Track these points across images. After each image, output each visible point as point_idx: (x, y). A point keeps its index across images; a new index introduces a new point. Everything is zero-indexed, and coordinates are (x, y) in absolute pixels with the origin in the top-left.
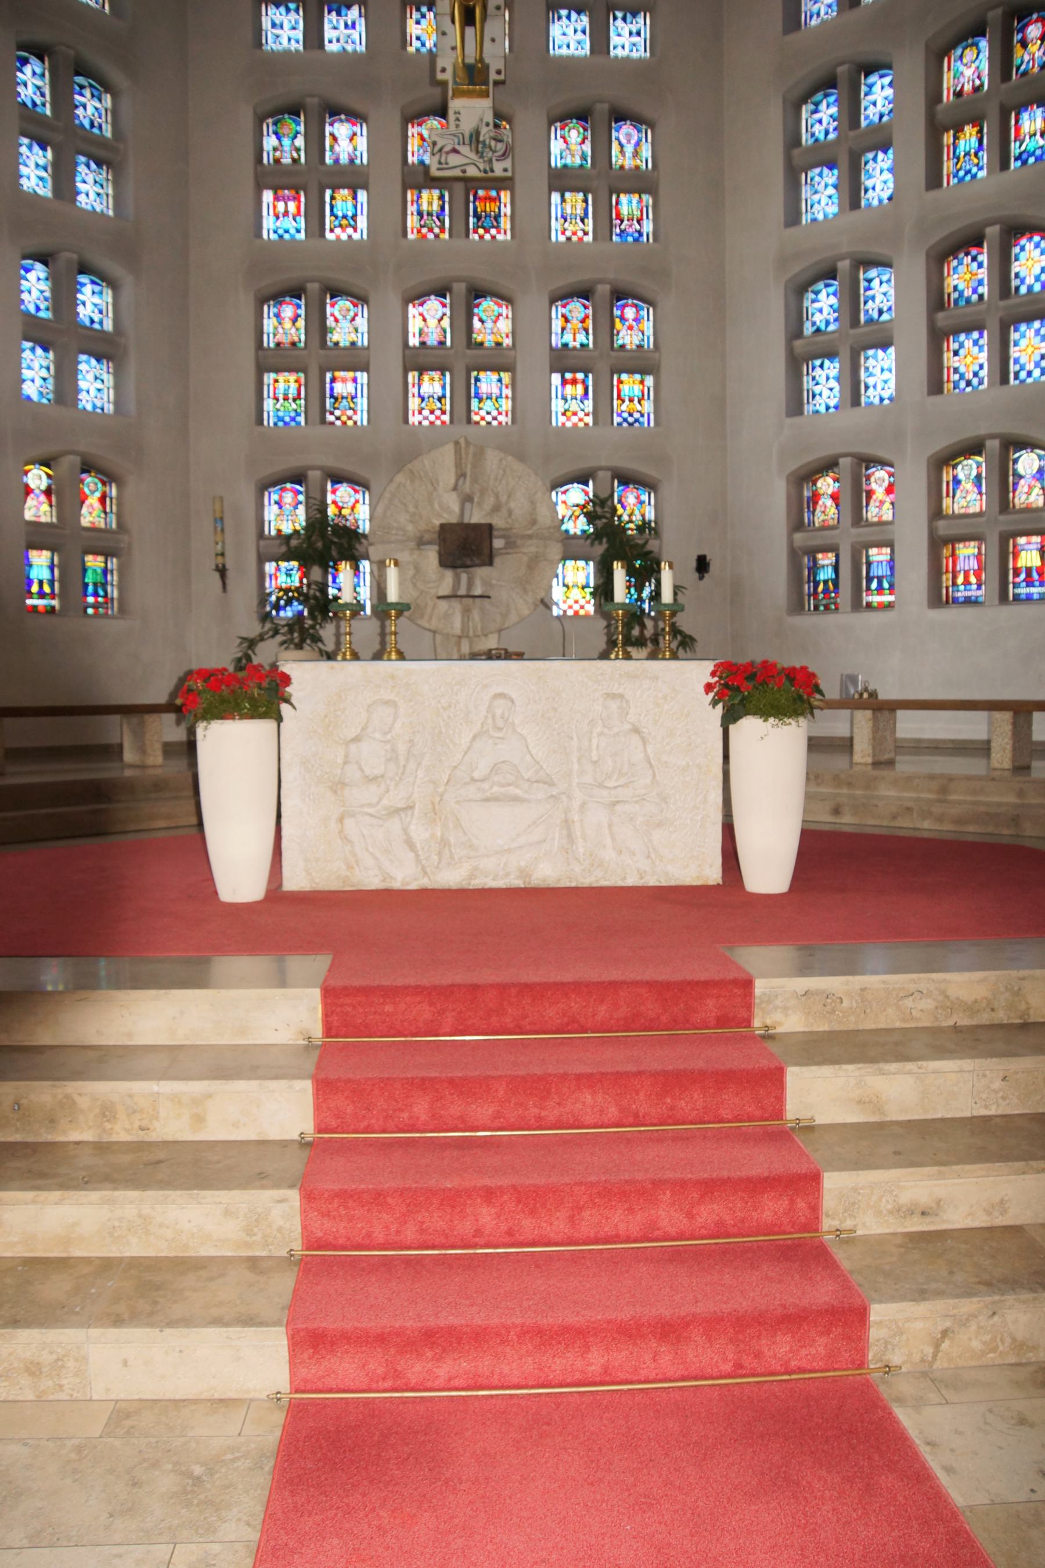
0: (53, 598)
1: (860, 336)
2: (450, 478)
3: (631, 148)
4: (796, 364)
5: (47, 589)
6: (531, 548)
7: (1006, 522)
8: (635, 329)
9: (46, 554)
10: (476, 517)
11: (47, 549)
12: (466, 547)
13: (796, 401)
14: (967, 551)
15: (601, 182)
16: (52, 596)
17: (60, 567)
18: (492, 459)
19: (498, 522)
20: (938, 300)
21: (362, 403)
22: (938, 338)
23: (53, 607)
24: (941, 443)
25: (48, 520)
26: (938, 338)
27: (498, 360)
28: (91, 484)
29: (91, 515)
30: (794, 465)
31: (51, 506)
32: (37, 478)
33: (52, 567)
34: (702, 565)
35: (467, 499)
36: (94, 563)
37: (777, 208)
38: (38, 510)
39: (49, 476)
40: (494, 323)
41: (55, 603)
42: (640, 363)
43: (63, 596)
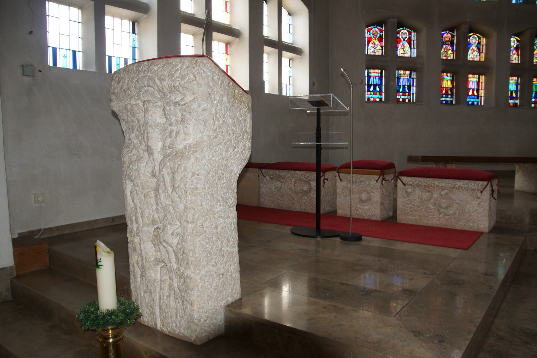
0: (517, 100)
5: (514, 95)
9: (515, 78)
11: (515, 76)
16: (516, 98)
17: (520, 84)
23: (516, 104)
25: (517, 62)
31: (518, 55)
32: (514, 42)
33: (517, 85)
38: (515, 58)
39: (518, 41)
41: (517, 102)
43: (521, 98)
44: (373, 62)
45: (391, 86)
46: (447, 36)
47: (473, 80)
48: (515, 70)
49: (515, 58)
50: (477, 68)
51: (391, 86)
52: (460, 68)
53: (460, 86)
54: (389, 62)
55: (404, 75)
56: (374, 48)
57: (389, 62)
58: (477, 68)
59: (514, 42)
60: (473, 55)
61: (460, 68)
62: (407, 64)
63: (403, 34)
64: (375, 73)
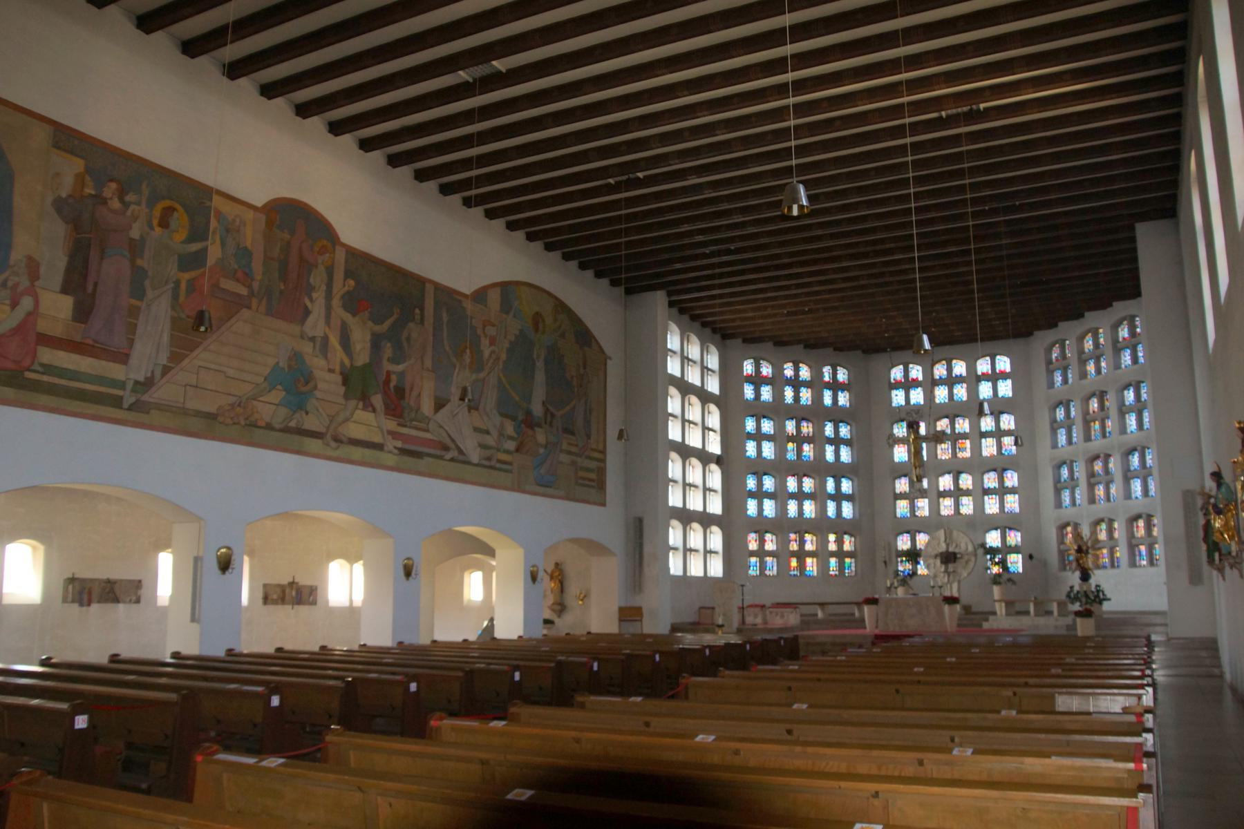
1: (1073, 483)
2: (943, 539)
3: (1008, 422)
4: (1058, 492)
6: (966, 558)
7: (1112, 543)
8: (1012, 479)
10: (951, 550)
12: (949, 558)
13: (1059, 504)
14: (1105, 551)
15: (998, 434)
18: (955, 533)
19: (957, 550)
20: (1091, 475)
21: (927, 508)
22: (1091, 487)
24: (1092, 519)
26: (1091, 487)
27: (967, 493)
28: (846, 538)
29: (848, 546)
30: (1058, 523)
32: (832, 537)
34: (1031, 557)
35: (948, 545)
36: (848, 560)
37: (1048, 442)
38: (832, 547)
40: (966, 481)
42: (1013, 491)
44: (752, 554)
45: (763, 566)
46: (793, 536)
47: (809, 561)
48: (833, 554)
49: (832, 547)
50: (812, 554)
51: (763, 566)
52: (801, 555)
53: (802, 566)
54: (761, 553)
55: (769, 559)
56: (753, 546)
57: (761, 553)
58: (812, 554)
59: (832, 537)
60: (809, 547)
61: (801, 555)
62: (771, 554)
63: (768, 536)
64: (753, 560)
